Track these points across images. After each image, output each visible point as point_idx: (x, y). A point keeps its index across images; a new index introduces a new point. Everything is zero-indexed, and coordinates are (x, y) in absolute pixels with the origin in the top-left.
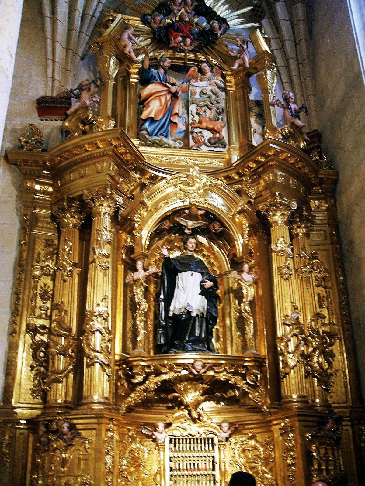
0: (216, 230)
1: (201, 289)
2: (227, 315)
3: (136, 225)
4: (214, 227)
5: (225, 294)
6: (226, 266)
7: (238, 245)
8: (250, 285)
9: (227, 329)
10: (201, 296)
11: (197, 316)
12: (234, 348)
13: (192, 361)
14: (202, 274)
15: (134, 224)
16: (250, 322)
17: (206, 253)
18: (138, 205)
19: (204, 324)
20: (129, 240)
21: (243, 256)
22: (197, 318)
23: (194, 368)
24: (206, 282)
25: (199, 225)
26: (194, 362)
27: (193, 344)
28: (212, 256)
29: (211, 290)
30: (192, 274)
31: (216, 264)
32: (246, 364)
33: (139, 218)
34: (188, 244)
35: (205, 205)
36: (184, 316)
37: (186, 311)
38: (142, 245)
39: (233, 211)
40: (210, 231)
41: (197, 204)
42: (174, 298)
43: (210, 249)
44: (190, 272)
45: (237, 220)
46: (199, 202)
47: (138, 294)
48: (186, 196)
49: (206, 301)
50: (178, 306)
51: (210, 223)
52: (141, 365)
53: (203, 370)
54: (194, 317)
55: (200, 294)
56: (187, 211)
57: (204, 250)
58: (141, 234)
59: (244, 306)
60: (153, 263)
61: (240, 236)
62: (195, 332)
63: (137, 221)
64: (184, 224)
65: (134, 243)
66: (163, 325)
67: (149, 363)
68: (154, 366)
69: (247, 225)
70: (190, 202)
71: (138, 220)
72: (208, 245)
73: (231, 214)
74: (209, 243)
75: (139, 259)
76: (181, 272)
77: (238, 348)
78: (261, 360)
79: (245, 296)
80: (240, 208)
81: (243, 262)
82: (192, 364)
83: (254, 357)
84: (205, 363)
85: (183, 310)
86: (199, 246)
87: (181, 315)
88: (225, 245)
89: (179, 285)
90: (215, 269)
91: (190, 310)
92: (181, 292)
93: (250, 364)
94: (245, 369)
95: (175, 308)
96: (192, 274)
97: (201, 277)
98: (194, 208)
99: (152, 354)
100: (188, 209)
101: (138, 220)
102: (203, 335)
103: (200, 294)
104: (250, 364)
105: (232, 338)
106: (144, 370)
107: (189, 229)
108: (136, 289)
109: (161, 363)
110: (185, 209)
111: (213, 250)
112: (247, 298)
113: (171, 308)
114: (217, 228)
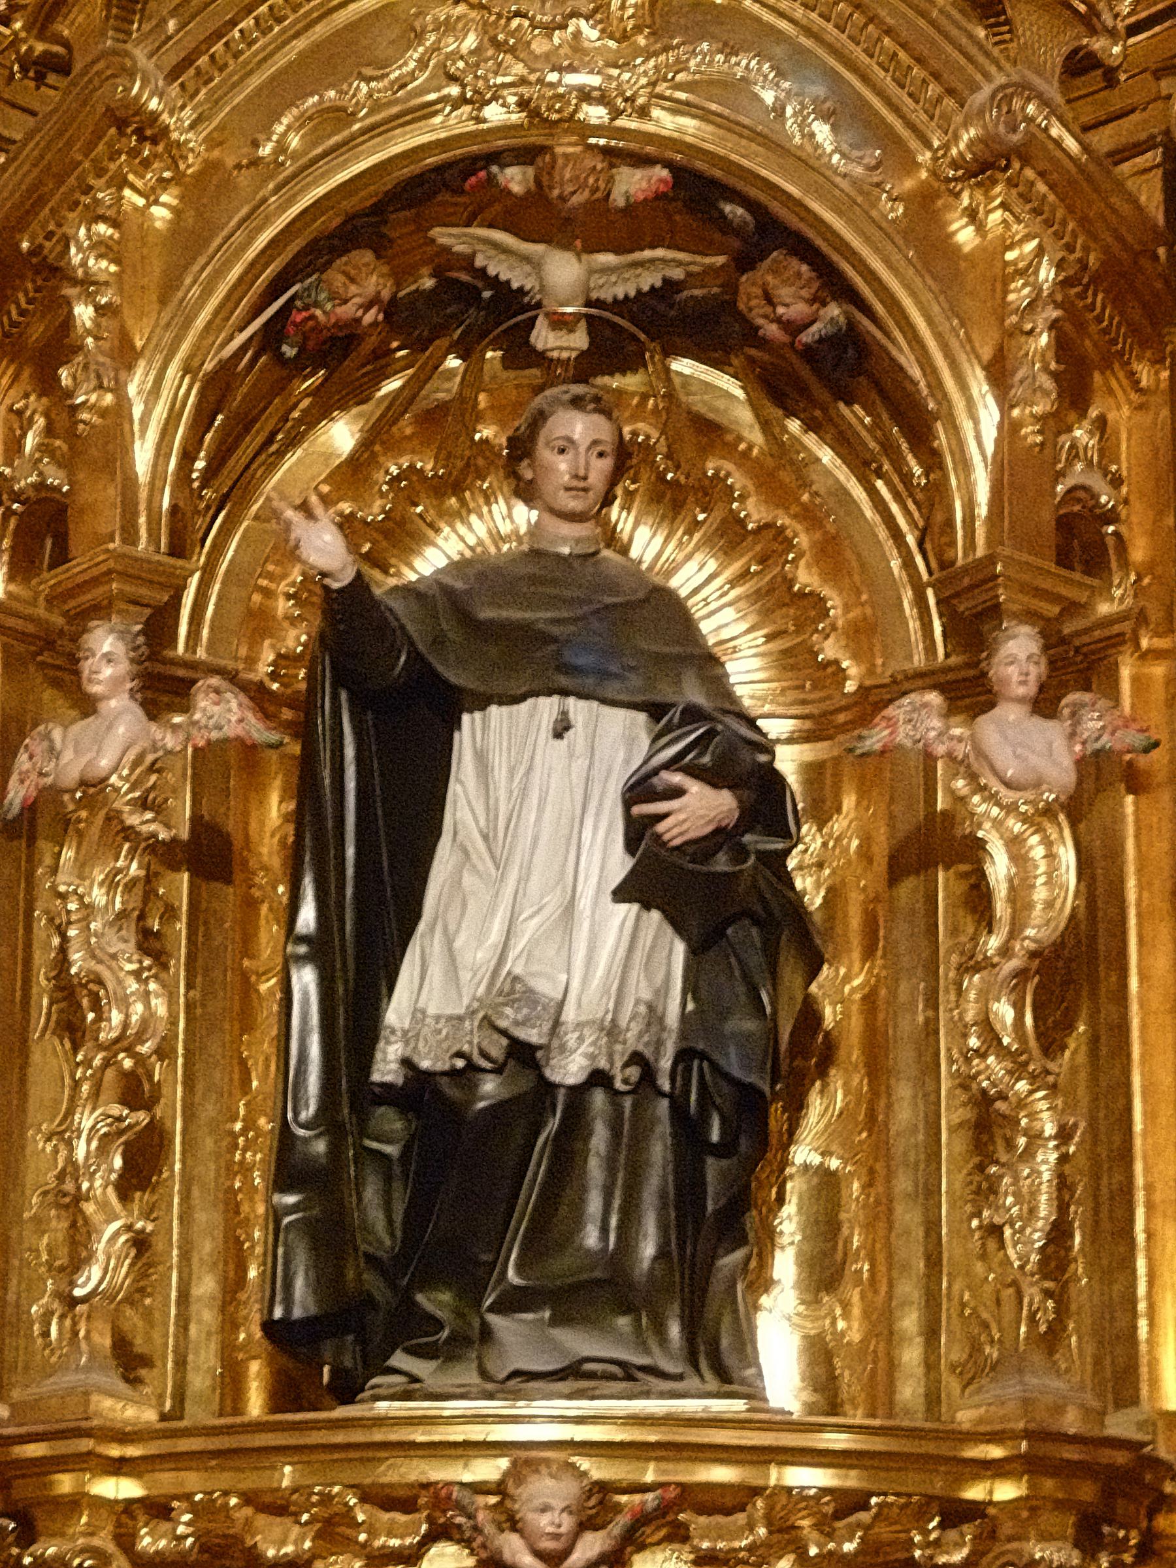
0: (794, 328)
1: (631, 846)
2: (904, 1057)
3: (84, 313)
4: (769, 299)
5: (897, 870)
6: (914, 625)
7: (965, 465)
8: (1048, 812)
9: (903, 1183)
10: (627, 911)
11: (598, 1078)
12: (951, 1350)
13: (489, 1470)
14: (656, 711)
15: (68, 304)
16: (1035, 1138)
17: (754, 512)
18: (98, 135)
19: (659, 1151)
20: (30, 441)
21: (991, 559)
22: (599, 1098)
23: (513, 1523)
24: (677, 792)
25: (649, 280)
26: (517, 1473)
27: (554, 1322)
28: (803, 540)
29: (721, 863)
30: (561, 729)
31: (835, 603)
32: (975, 1492)
33: (103, 248)
34: (545, 454)
35: (665, 122)
36: (489, 1086)
37: (497, 1048)
38: (130, 481)
39: (925, 157)
40: (752, 334)
41: (595, 114)
42: (422, 926)
43: (786, 476)
44: (547, 708)
45: (965, 236)
46: (603, 99)
47: (88, 910)
48: (498, 46)
49: (680, 948)
50: (437, 1003)
51: (745, 262)
52: (100, 1503)
53: (591, 1546)
54: (578, 1093)
55: (621, 894)
56: (515, 179)
57: (737, 480)
58: (119, 390)
59: (985, 997)
60: (283, 606)
61: (980, 386)
62: (578, 1221)
63: (88, 284)
64: (516, 277)
65: (65, 463)
66: (310, 1159)
67: (166, 1481)
68: (194, 1508)
69: (1047, 274)
70: (523, 104)
71: (102, 267)
72: (756, 437)
73: (909, 184)
74: (765, 425)
75: (100, 611)
76: (482, 702)
77: (975, 1348)
78: (1121, 1458)
79: (1001, 908)
80: (970, 134)
81: (994, 612)
82: (499, 1488)
83: (1028, 1434)
84: (603, 1488)
85: (471, 1040)
86: (688, 452)
87: (467, 1074)
88: (889, 449)
89: (464, 814)
90: (830, 650)
91: (532, 1035)
92: (468, 880)
93: (1006, 1491)
94: (969, 1532)
95: (419, 1015)
96: (561, 729)
97: (644, 742)
98: (566, 147)
99: (255, 1404)
100: (527, 155)
101: (102, 267)
102: (648, 1249)
103: (621, 894)
104: (1006, 1491)
105: (934, 1261)
106: (126, 1541)
107: (560, 323)
108: (82, 869)
109: (251, 1481)
110: (495, 157)
111: (806, 484)
112: (1015, 932)
113: (396, 1013)
114: (797, 310)
